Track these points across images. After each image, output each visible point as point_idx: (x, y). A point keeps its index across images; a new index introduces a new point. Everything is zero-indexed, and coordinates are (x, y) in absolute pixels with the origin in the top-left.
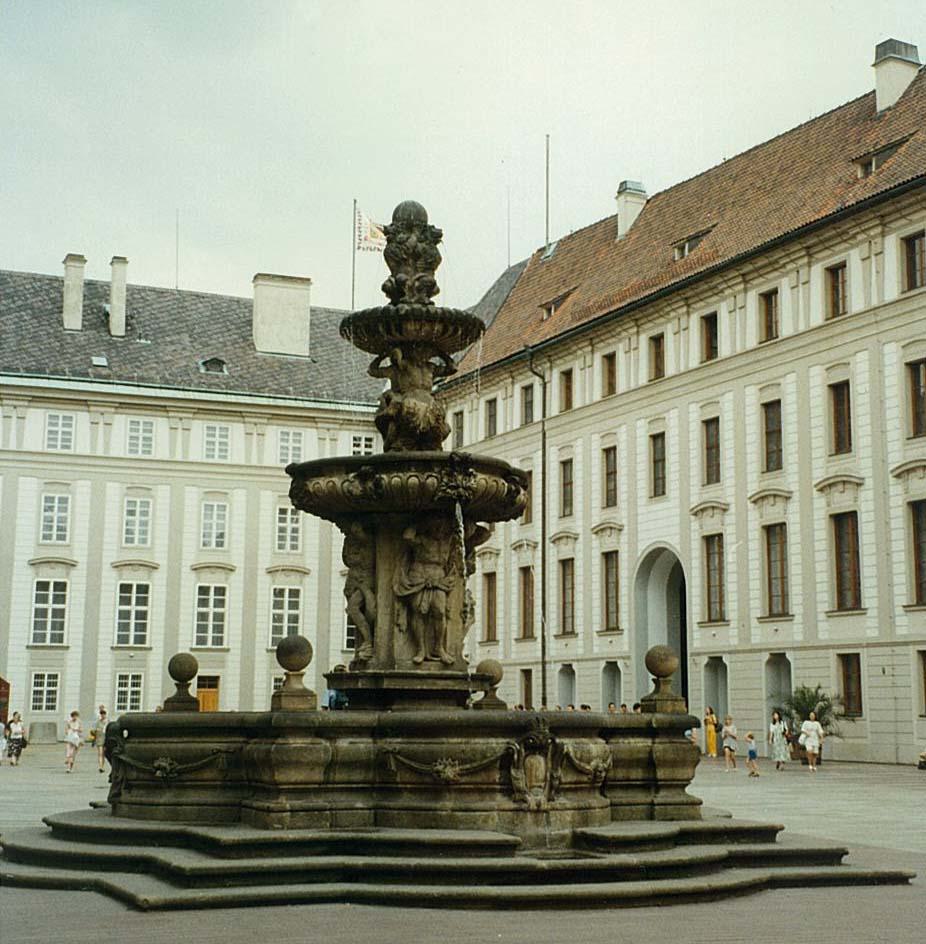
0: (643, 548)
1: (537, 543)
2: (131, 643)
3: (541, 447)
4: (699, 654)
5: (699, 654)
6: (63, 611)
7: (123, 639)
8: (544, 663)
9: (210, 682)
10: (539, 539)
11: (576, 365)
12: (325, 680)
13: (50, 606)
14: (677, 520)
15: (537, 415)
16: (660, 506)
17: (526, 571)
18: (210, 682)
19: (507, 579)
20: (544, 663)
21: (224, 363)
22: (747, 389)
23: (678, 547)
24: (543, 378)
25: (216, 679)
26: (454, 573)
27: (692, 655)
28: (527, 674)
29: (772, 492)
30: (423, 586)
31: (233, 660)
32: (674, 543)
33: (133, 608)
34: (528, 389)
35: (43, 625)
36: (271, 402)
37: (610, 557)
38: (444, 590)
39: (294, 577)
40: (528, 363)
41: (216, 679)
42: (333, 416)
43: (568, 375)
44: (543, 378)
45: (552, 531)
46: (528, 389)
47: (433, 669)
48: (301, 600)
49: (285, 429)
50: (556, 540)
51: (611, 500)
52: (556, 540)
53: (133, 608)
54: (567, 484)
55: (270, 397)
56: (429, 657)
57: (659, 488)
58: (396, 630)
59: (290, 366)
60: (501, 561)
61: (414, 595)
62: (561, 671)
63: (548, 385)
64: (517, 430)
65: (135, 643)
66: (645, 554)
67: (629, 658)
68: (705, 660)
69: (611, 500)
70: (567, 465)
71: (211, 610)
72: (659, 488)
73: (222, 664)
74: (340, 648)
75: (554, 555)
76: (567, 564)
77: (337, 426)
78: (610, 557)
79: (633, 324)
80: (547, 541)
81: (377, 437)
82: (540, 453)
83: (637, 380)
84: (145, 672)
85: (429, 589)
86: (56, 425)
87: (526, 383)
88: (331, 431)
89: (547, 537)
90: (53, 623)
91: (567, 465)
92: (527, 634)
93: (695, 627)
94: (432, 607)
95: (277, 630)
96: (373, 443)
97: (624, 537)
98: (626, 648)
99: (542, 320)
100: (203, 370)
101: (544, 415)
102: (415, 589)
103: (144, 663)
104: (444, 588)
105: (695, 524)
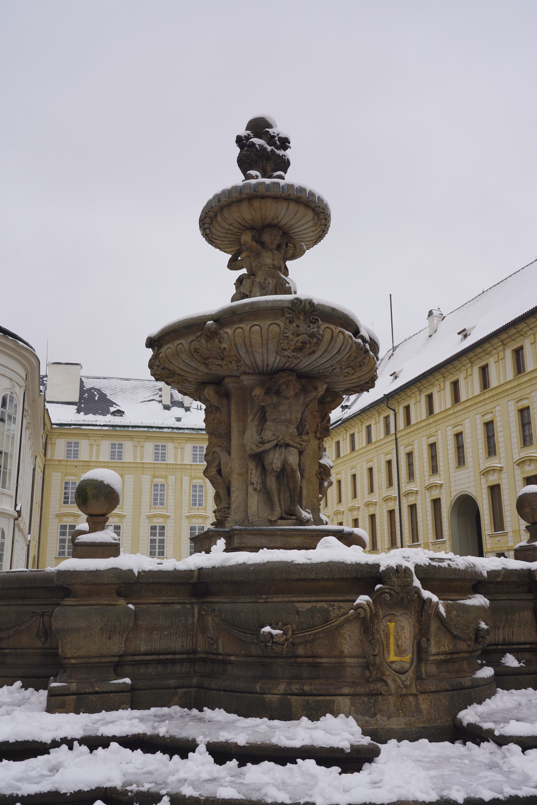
3: (395, 447)
6: (164, 540)
11: (412, 402)
13: (157, 538)
15: (392, 430)
17: (391, 513)
22: (509, 403)
24: (394, 411)
26: (307, 433)
29: (529, 458)
30: (275, 443)
34: (387, 418)
35: (160, 547)
37: (436, 503)
38: (296, 448)
40: (386, 404)
43: (407, 409)
44: (394, 411)
45: (403, 490)
46: (387, 418)
54: (410, 465)
56: (285, 516)
57: (461, 460)
58: (251, 489)
61: (266, 452)
63: (397, 415)
69: (434, 470)
70: (410, 455)
72: (461, 460)
76: (413, 508)
78: (436, 503)
80: (401, 496)
82: (395, 450)
85: (281, 446)
86: (158, 449)
89: (401, 493)
90: (159, 546)
91: (410, 455)
94: (285, 464)
101: (396, 430)
102: (267, 446)
104: (295, 445)
105: (483, 481)
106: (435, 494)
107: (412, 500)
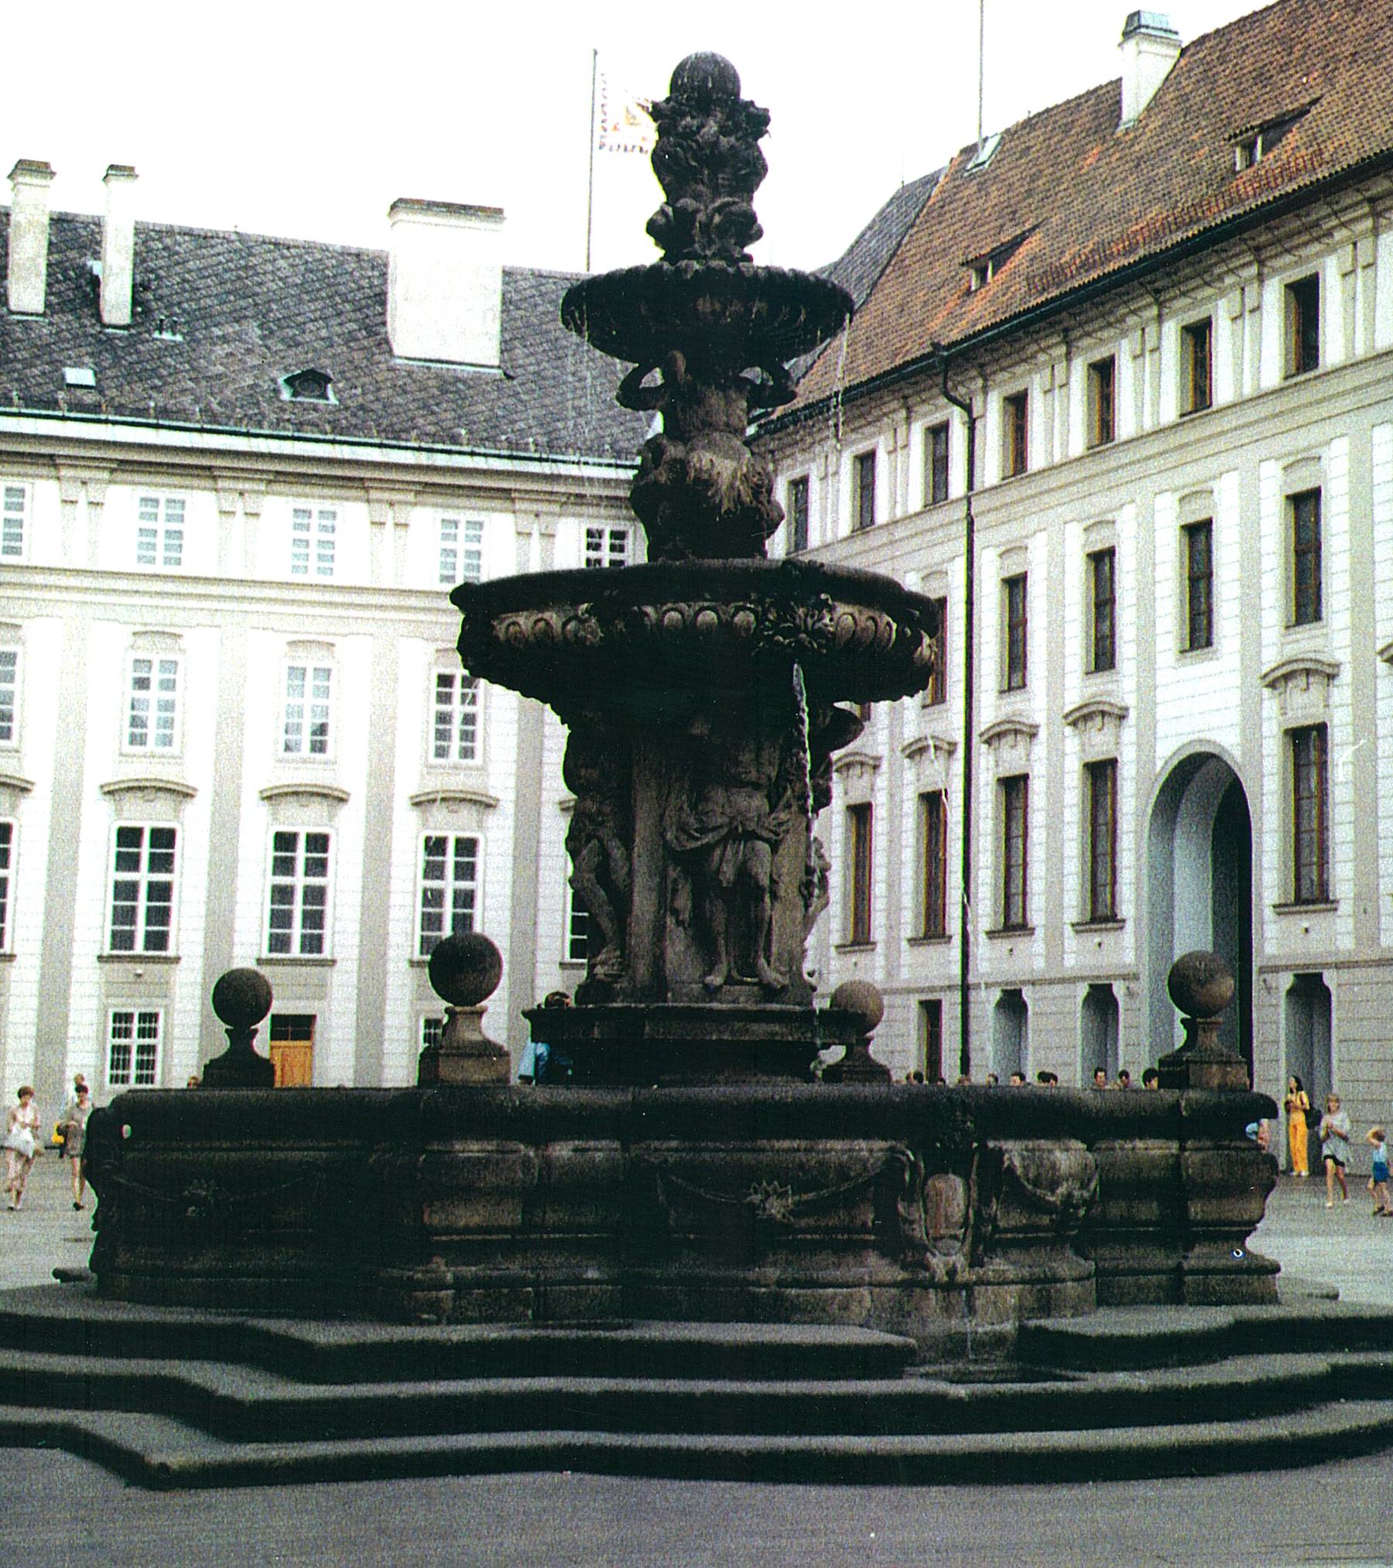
0: (1167, 751)
1: (953, 745)
2: (139, 948)
3: (964, 549)
4: (1275, 969)
5: (1275, 969)
7: (123, 940)
8: (965, 988)
9: (298, 1028)
10: (960, 737)
12: (528, 1023)
14: (1235, 698)
15: (957, 485)
16: (1201, 669)
17: (932, 802)
18: (298, 1028)
19: (894, 816)
20: (965, 988)
21: (328, 380)
23: (1237, 753)
24: (968, 408)
25: (310, 1020)
26: (789, 806)
27: (1262, 970)
28: (932, 1010)
31: (343, 983)
32: (1228, 740)
33: (143, 876)
34: (938, 433)
36: (424, 459)
39: (466, 814)
40: (940, 380)
41: (310, 1020)
42: (548, 488)
43: (1018, 404)
44: (968, 408)
46: (938, 433)
47: (743, 999)
48: (479, 860)
49: (450, 515)
50: (994, 737)
51: (1103, 657)
52: (994, 737)
53: (143, 876)
55: (420, 449)
58: (670, 921)
59: (460, 386)
60: (882, 781)
61: (709, 848)
62: (1000, 1005)
63: (979, 425)
64: (917, 514)
65: (147, 948)
66: (1170, 768)
67: (1136, 977)
68: (1286, 981)
69: (1103, 657)
70: (1016, 585)
71: (300, 880)
73: (321, 990)
74: (559, 959)
75: (988, 770)
77: (556, 508)
79: (1149, 299)
80: (975, 739)
81: (635, 532)
82: (961, 563)
83: (1156, 413)
84: (166, 1006)
87: (936, 418)
88: (543, 518)
91: (1016, 585)
92: (933, 930)
93: (1269, 913)
94: (744, 873)
95: (431, 921)
96: (629, 543)
97: (1129, 733)
98: (1129, 957)
99: (969, 292)
100: (286, 395)
103: (164, 989)
104: (765, 834)
105: (1270, 705)
106: (1100, 743)
107: (1011, 759)
